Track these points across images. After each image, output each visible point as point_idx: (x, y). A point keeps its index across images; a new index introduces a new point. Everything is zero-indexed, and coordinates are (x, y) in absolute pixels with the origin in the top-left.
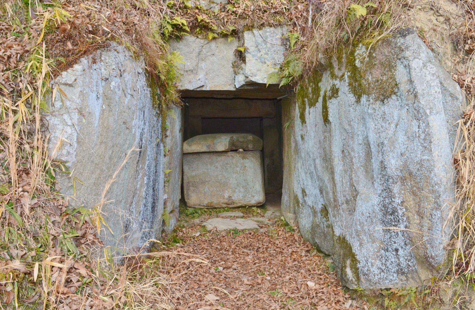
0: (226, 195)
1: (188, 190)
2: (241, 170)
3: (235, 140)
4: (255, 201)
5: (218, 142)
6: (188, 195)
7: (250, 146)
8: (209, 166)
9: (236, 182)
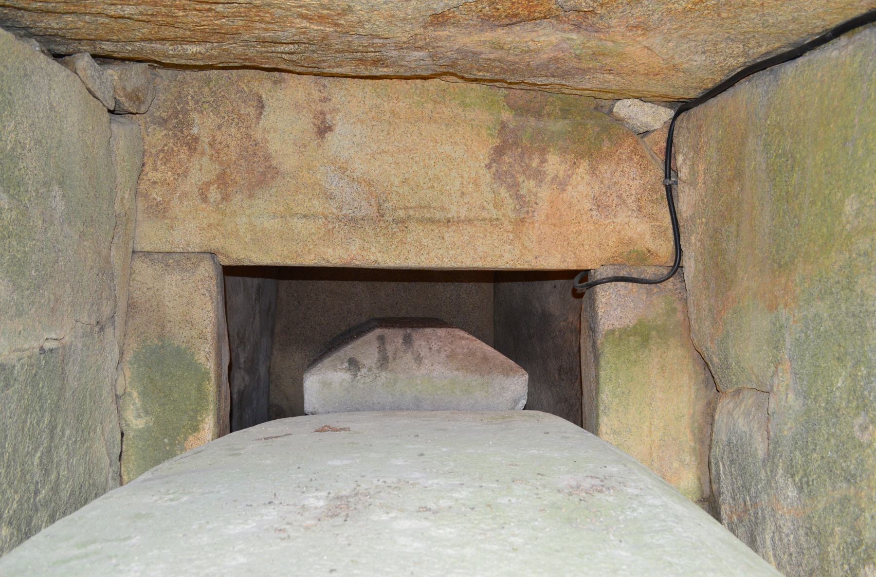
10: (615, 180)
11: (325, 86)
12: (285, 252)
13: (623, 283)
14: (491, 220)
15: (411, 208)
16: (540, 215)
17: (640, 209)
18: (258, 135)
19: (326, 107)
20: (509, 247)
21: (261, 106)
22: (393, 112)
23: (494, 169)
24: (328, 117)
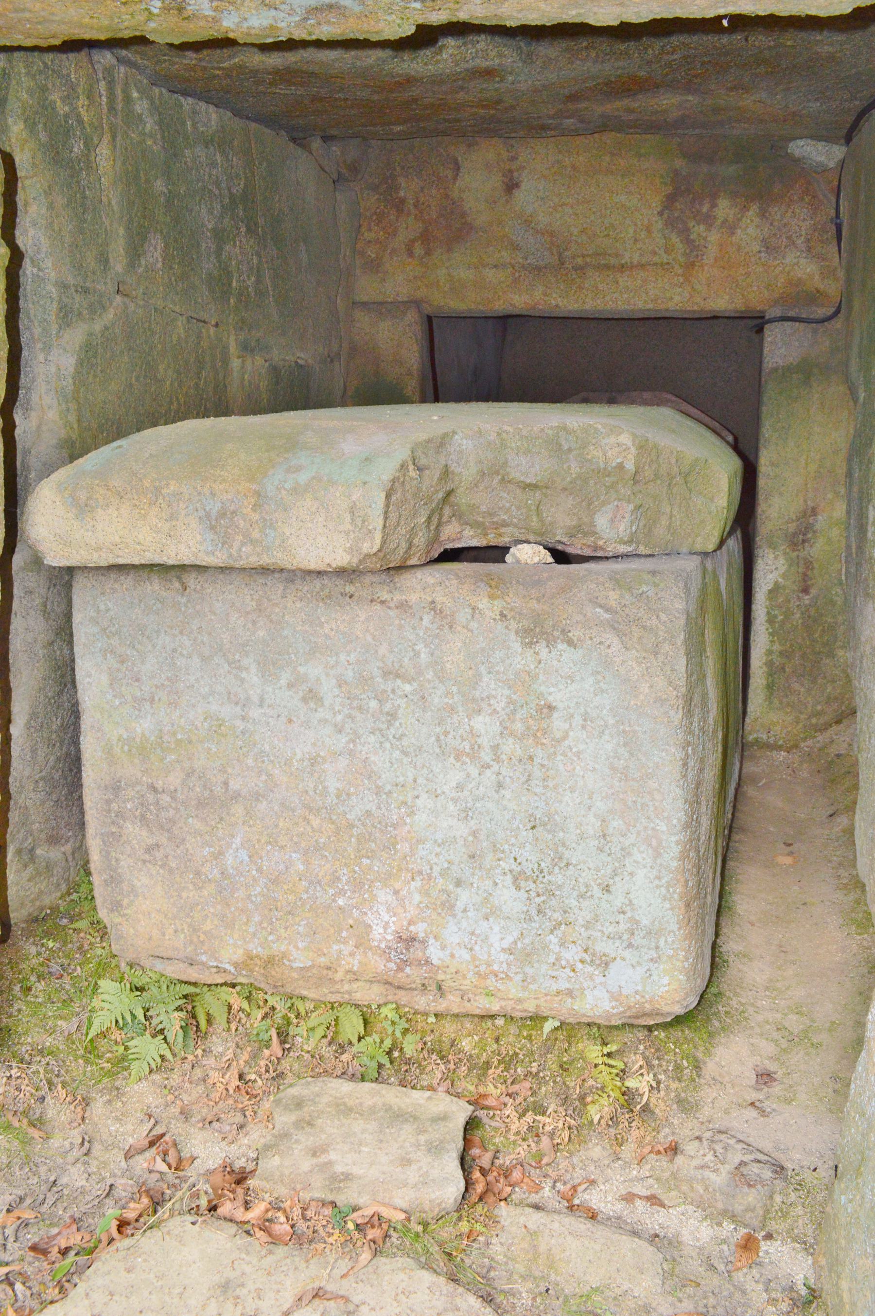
0: (383, 925)
1: (112, 839)
2: (506, 731)
3: (466, 472)
4: (615, 997)
5: (296, 491)
6: (114, 880)
7: (611, 526)
8: (253, 677)
9: (462, 830)
10: (785, 221)
11: (512, 146)
12: (479, 299)
13: (789, 323)
14: (662, 264)
15: (588, 256)
16: (709, 259)
17: (809, 249)
18: (455, 194)
19: (515, 165)
20: (679, 290)
21: (457, 168)
22: (574, 167)
23: (666, 216)
24: (516, 174)
